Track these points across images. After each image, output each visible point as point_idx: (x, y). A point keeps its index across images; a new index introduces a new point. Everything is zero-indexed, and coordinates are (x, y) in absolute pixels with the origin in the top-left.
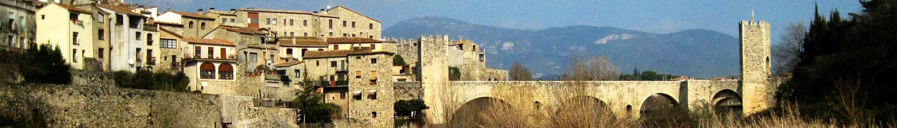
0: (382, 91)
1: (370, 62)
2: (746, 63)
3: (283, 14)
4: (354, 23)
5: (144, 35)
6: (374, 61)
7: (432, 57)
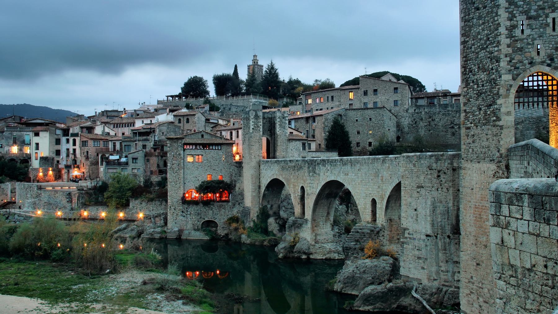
2: (465, 104)
3: (326, 92)
4: (375, 91)
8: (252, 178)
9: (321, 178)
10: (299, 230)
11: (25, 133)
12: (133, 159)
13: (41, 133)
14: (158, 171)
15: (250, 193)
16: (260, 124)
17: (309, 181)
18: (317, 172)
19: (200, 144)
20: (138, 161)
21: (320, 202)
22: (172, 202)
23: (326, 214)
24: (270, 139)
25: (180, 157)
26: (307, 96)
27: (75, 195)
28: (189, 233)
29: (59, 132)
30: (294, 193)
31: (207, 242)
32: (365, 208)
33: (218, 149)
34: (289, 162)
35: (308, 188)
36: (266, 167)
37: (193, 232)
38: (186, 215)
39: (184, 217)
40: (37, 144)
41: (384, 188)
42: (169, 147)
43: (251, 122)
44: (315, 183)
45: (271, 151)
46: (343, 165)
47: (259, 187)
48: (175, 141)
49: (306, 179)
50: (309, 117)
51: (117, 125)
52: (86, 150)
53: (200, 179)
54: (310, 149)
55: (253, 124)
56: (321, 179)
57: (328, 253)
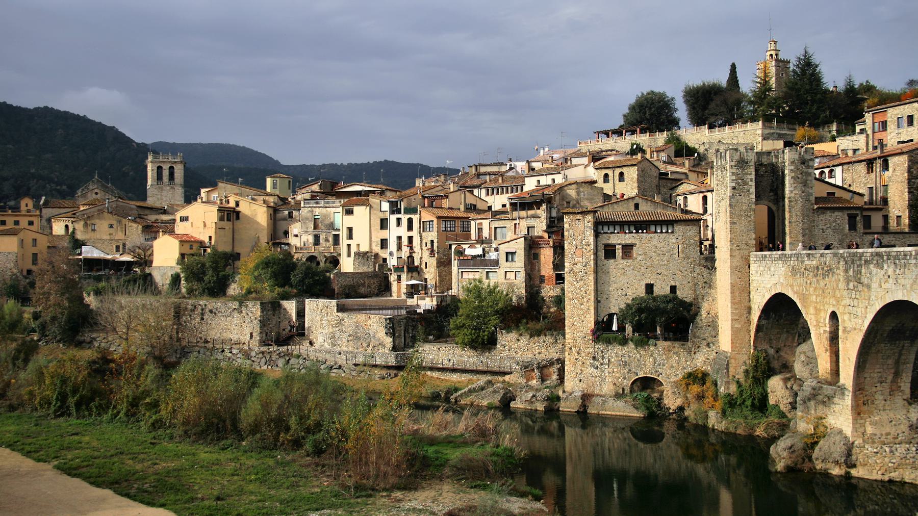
5: (405, 218)
8: (732, 292)
9: (873, 294)
10: (826, 410)
11: (333, 210)
12: (507, 254)
13: (356, 209)
14: (554, 275)
15: (730, 322)
16: (749, 177)
17: (847, 301)
18: (865, 280)
19: (629, 223)
20: (516, 258)
21: (873, 348)
22: (574, 339)
23: (890, 378)
24: (774, 208)
25: (588, 249)
26: (875, 115)
27: (399, 322)
28: (604, 402)
29: (386, 206)
30: (817, 326)
31: (638, 422)
33: (667, 232)
34: (806, 259)
35: (846, 317)
36: (762, 269)
37: (611, 402)
38: (602, 364)
39: (597, 368)
40: (350, 230)
42: (568, 231)
43: (728, 175)
44: (860, 303)
45: (776, 234)
47: (749, 310)
48: (579, 217)
49: (842, 296)
50: (875, 159)
51: (493, 190)
52: (430, 239)
53: (630, 292)
54: (870, 227)
55: (734, 178)
56: (872, 297)
57: (895, 469)
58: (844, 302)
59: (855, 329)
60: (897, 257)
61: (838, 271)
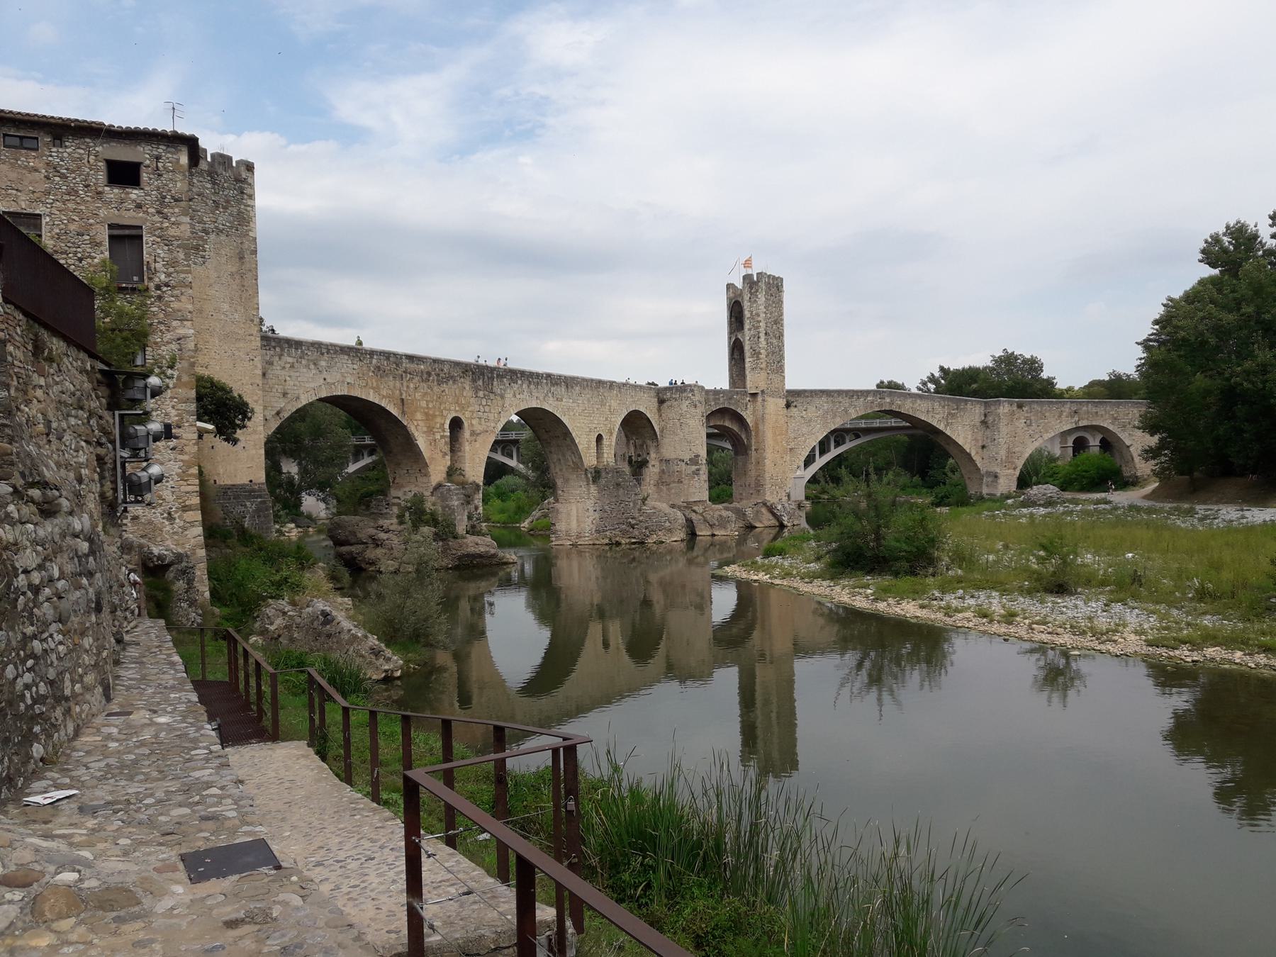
0: (181, 331)
1: (102, 176)
6: (125, 175)
7: (207, 233)
32: (588, 448)
41: (613, 420)
44: (492, 411)
46: (553, 385)
58: (470, 409)
59: (487, 431)
60: (528, 377)
61: (462, 380)
